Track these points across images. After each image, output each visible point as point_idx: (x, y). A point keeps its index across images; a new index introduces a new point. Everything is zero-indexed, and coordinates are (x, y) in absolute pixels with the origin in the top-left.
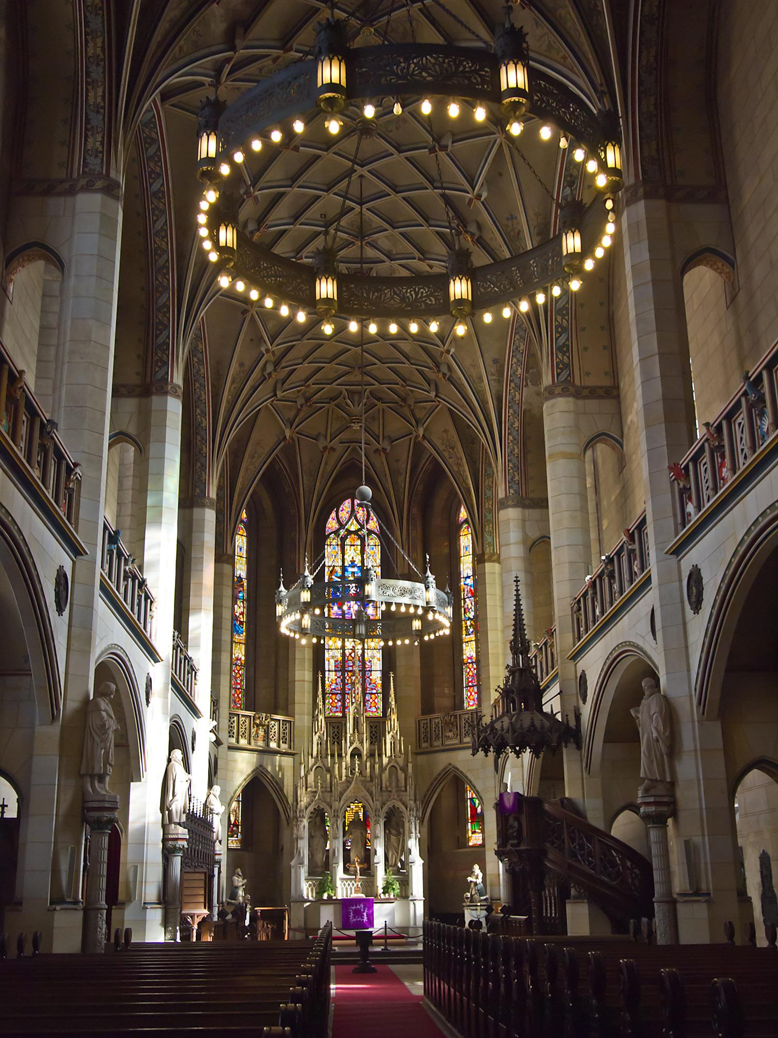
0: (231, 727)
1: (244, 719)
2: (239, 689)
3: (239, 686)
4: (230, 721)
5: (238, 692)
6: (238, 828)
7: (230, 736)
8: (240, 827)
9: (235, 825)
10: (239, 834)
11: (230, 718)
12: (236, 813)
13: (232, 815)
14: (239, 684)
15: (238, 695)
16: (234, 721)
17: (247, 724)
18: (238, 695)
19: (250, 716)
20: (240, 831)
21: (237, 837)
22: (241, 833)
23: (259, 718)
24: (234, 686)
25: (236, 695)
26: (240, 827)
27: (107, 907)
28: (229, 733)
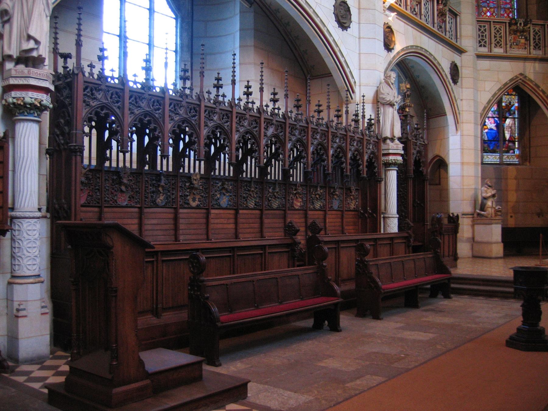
0: (482, 36)
1: (498, 26)
2: (508, 9)
3: (509, 6)
4: (480, 30)
5: (508, 12)
6: (515, 144)
7: (480, 46)
8: (517, 143)
9: (512, 140)
10: (516, 150)
11: (481, 26)
12: (512, 130)
13: (506, 132)
14: (508, 4)
15: (508, 15)
16: (485, 30)
17: (502, 32)
18: (508, 15)
19: (506, 23)
20: (517, 146)
21: (514, 152)
22: (518, 149)
23: (516, 24)
24: (502, 6)
25: (506, 15)
26: (517, 143)
27: (398, 216)
28: (480, 42)
